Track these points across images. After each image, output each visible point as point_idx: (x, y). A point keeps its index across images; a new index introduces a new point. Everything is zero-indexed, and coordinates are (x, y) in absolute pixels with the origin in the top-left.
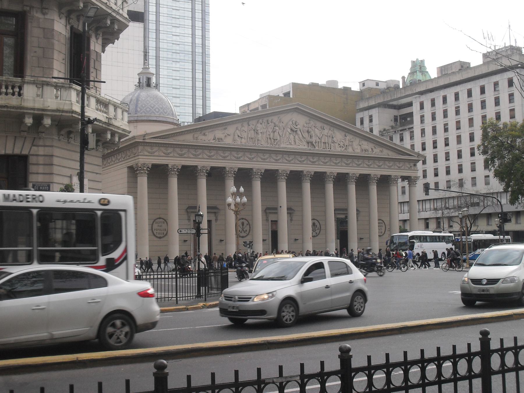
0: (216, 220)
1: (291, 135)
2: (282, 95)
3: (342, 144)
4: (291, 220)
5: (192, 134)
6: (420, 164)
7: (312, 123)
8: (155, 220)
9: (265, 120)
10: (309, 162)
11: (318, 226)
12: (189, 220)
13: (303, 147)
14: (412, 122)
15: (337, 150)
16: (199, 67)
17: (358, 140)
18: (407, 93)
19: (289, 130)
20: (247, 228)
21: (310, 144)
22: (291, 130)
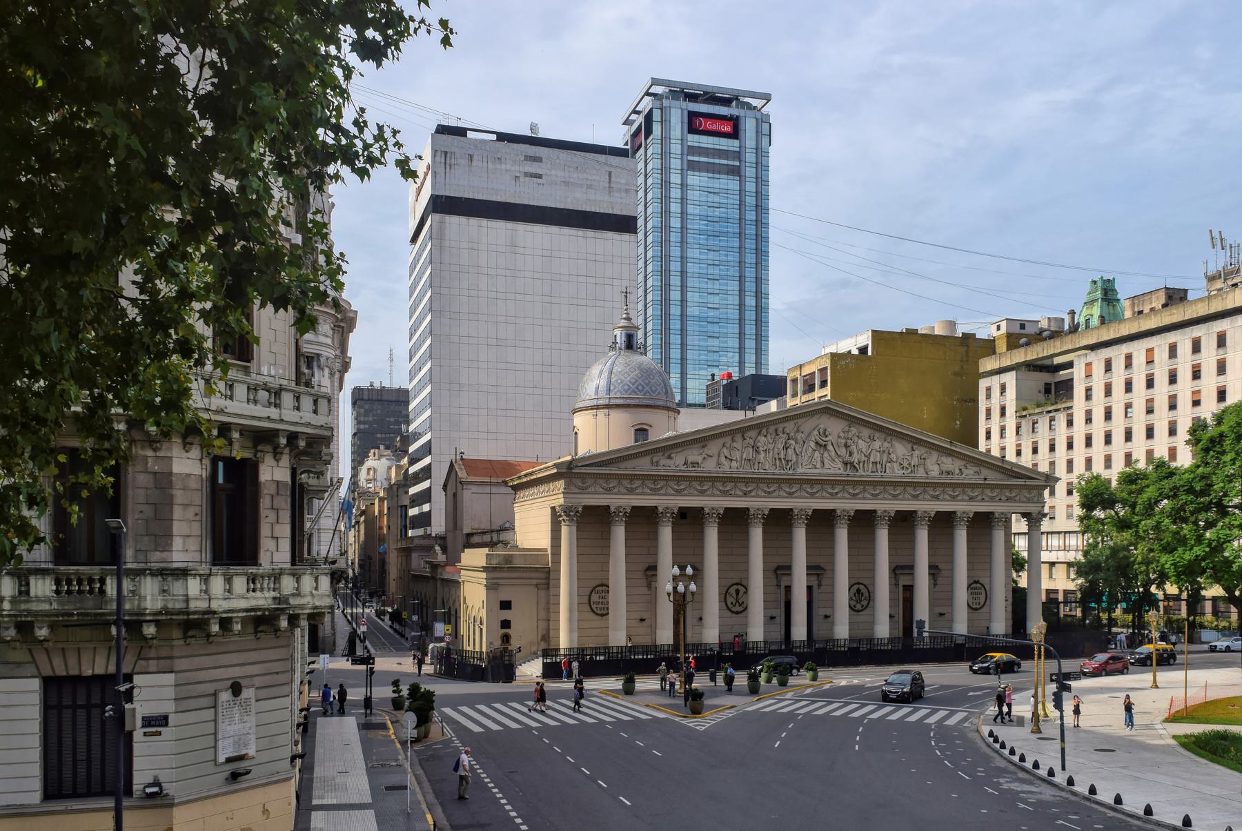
1: (817, 454)
2: (855, 352)
3: (905, 465)
4: (819, 585)
6: (1046, 492)
7: (854, 430)
9: (772, 429)
10: (846, 495)
11: (866, 594)
13: (834, 469)
14: (1070, 396)
15: (895, 472)
16: (750, 286)
17: (935, 455)
18: (1065, 348)
19: (813, 444)
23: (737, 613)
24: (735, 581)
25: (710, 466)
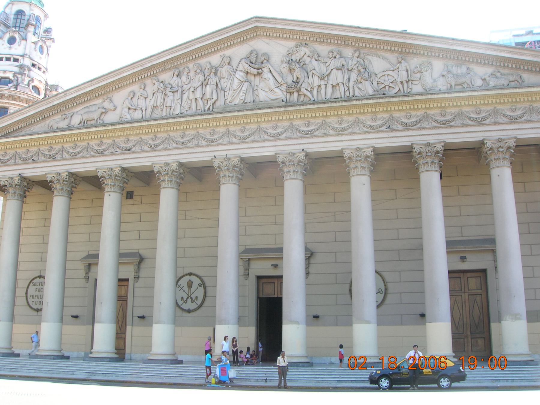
0: (137, 278)
5: (47, 122)
7: (304, 50)
8: (33, 279)
9: (191, 66)
12: (87, 278)
19: (240, 75)
20: (199, 293)
21: (296, 94)
22: (247, 73)
23: (189, 311)
24: (187, 271)
25: (110, 117)
